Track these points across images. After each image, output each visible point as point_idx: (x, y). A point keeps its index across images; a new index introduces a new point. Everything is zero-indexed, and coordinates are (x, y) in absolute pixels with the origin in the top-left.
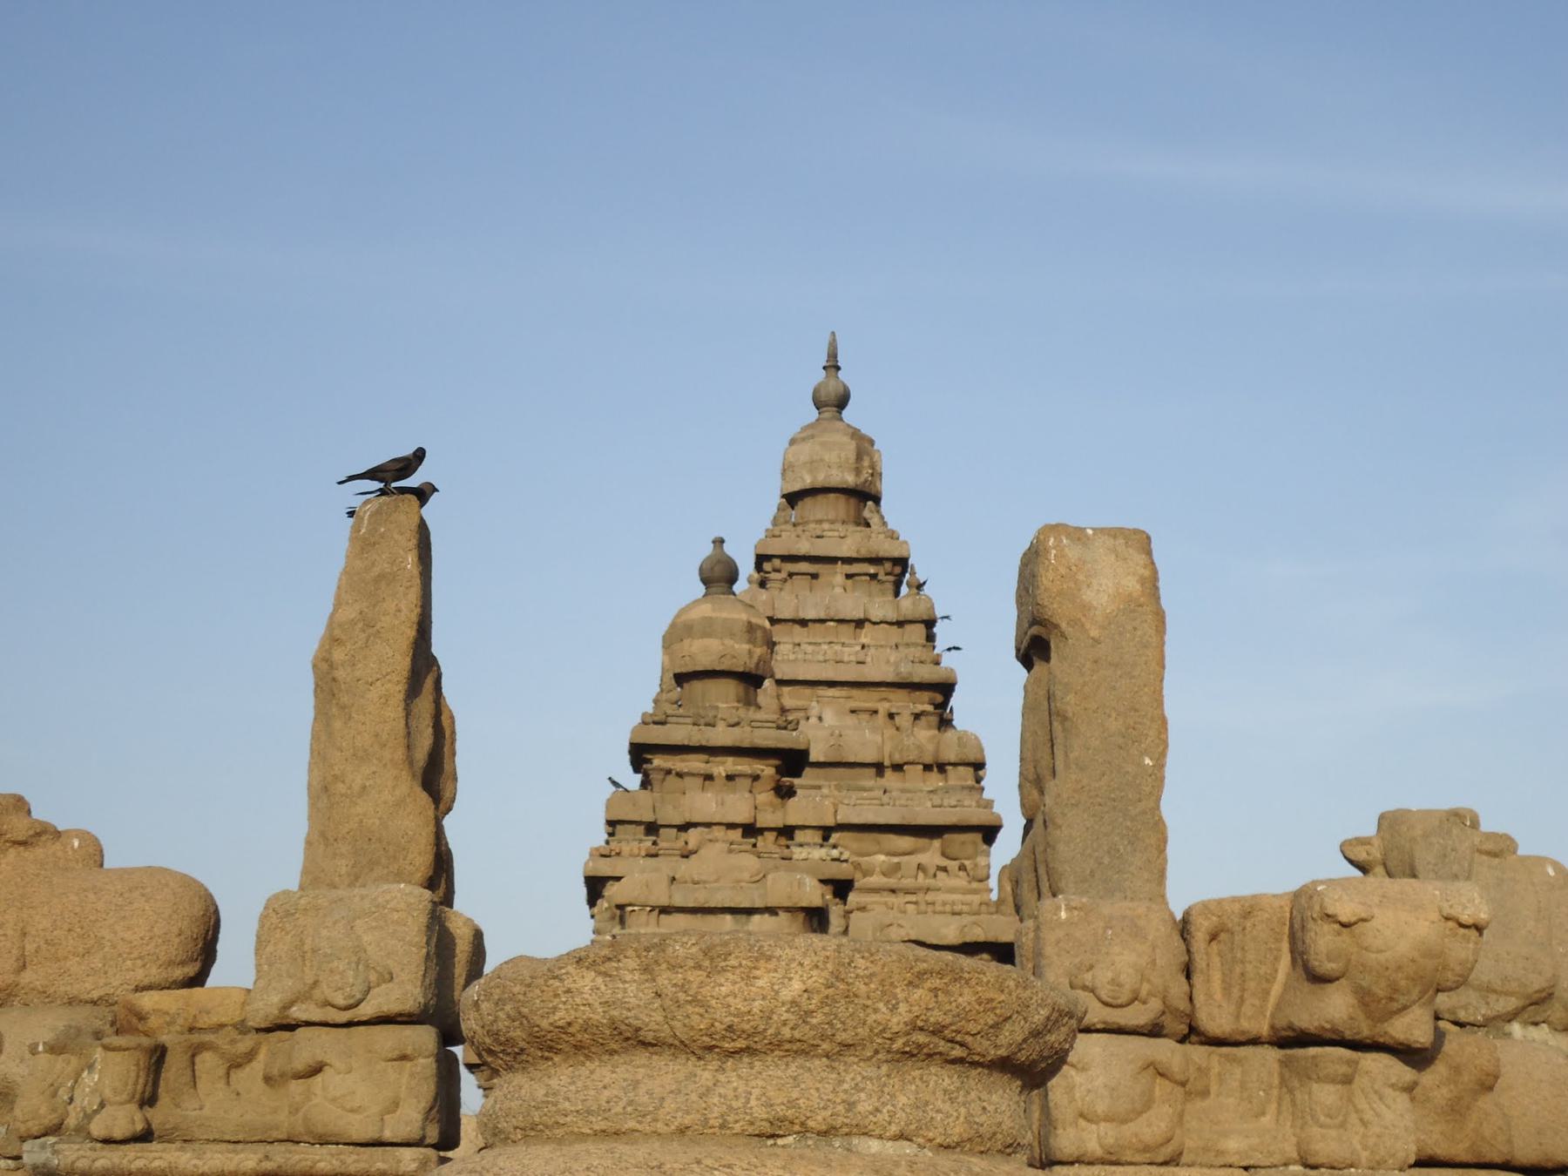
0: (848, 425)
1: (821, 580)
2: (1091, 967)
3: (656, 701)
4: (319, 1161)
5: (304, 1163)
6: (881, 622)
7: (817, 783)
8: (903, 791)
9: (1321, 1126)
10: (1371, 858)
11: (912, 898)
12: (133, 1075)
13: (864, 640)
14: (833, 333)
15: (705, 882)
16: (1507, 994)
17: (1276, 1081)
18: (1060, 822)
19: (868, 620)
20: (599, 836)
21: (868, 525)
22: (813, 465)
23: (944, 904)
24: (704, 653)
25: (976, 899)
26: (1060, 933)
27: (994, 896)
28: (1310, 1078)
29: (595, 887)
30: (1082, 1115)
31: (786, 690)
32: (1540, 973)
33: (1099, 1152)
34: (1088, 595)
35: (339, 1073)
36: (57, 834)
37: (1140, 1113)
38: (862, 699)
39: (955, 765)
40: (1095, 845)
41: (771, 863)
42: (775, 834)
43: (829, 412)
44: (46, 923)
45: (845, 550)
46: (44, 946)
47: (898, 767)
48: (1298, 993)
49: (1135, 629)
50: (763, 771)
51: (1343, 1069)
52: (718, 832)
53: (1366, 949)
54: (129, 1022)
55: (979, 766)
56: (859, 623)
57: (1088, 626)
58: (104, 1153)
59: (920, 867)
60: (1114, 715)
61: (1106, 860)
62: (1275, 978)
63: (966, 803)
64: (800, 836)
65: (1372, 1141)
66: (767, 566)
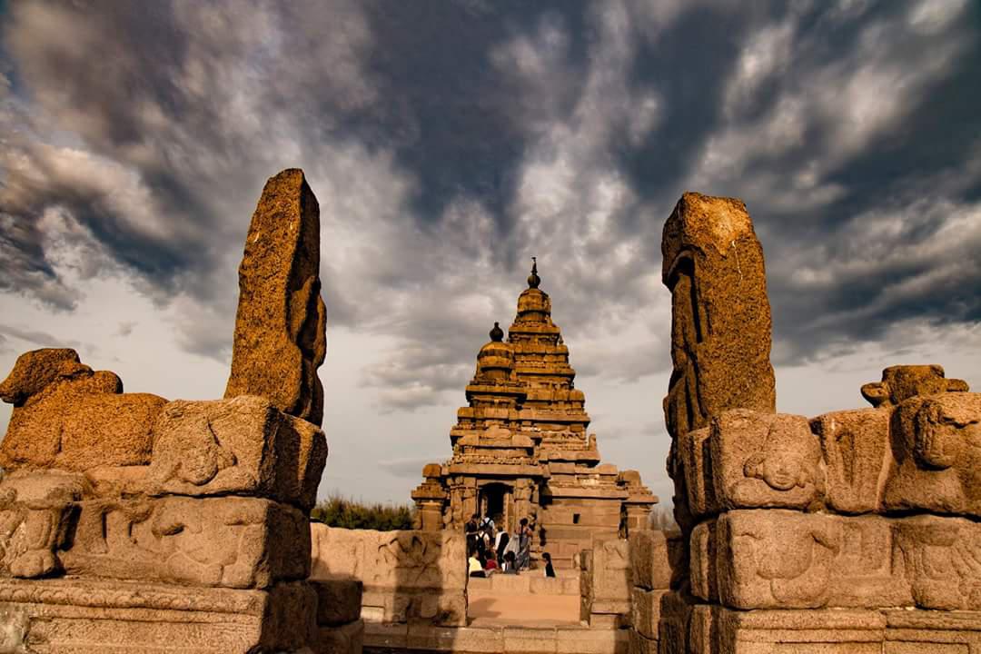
3: (475, 377)
4: (176, 598)
5: (164, 600)
9: (933, 578)
10: (882, 395)
12: (46, 528)
13: (545, 360)
17: (888, 541)
20: (455, 422)
25: (581, 446)
26: (735, 436)
28: (924, 542)
29: (454, 439)
30: (758, 573)
33: (773, 602)
34: (717, 231)
35: (192, 533)
36: (91, 373)
37: (802, 572)
40: (731, 383)
44: (74, 424)
45: (539, 330)
46: (71, 439)
48: (909, 478)
49: (746, 251)
53: (974, 445)
55: (583, 402)
57: (718, 248)
58: (21, 586)
59: (563, 435)
60: (738, 301)
61: (739, 392)
62: (881, 467)
64: (524, 423)
65: (969, 589)
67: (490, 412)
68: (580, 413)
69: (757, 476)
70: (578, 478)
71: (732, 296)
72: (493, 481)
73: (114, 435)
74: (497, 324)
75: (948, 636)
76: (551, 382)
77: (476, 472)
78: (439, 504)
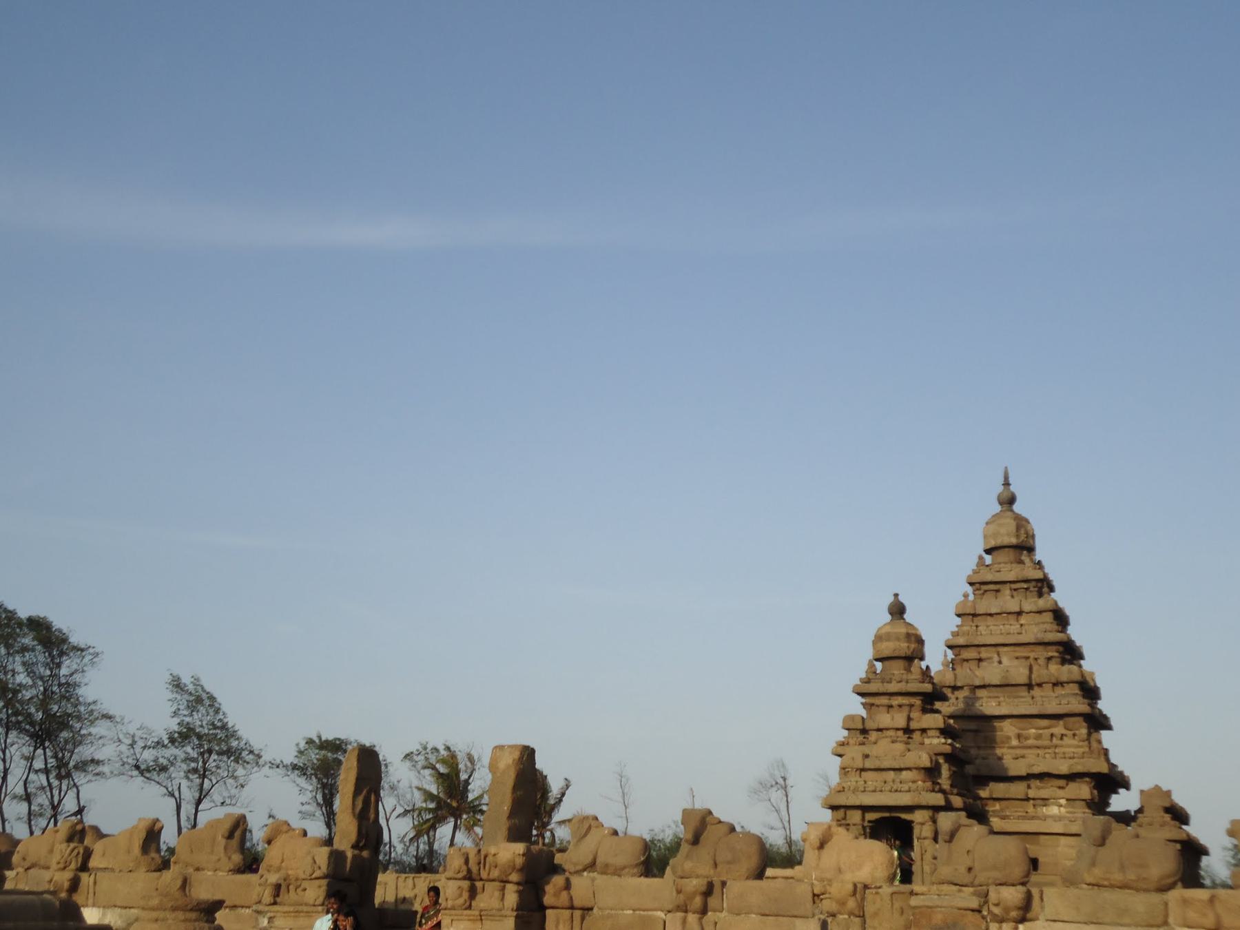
6: (1031, 612)
7: (996, 695)
13: (1022, 622)
14: (1006, 468)
19: (1023, 612)
22: (995, 535)
23: (1064, 753)
24: (888, 648)
31: (983, 649)
38: (1022, 652)
39: (1068, 683)
43: (1005, 508)
45: (1011, 577)
47: (1040, 685)
52: (891, 733)
56: (1019, 613)
59: (1052, 735)
64: (930, 733)
67: (885, 719)
70: (1034, 806)
72: (887, 815)
74: (896, 595)
75: (497, 918)
76: (1032, 655)
77: (858, 803)
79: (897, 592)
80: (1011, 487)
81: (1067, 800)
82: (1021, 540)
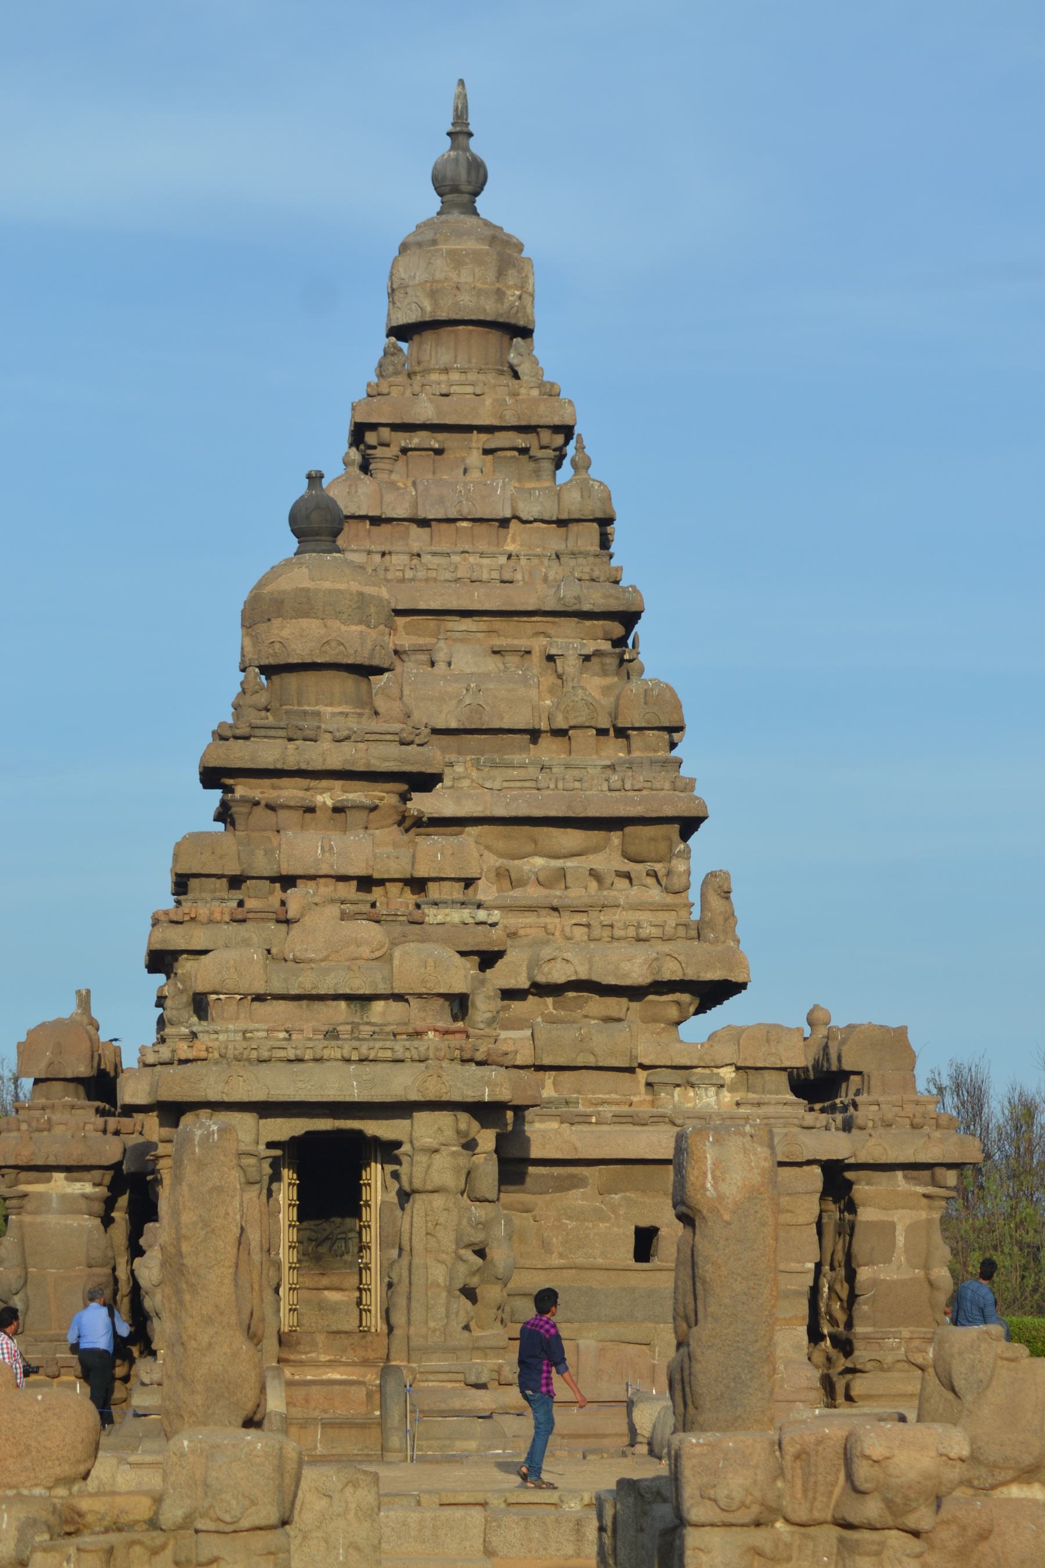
0: (487, 224)
1: (448, 456)
2: (714, 1486)
3: (236, 707)
6: (536, 520)
8: (568, 767)
11: (583, 919)
13: (510, 547)
14: (461, 82)
15: (311, 961)
16: (1008, 1468)
17: (835, 1550)
18: (700, 1358)
19: (516, 517)
21: (516, 375)
25: (671, 919)
26: (695, 1461)
27: (696, 915)
32: (1030, 1454)
40: (725, 1375)
41: (397, 930)
42: (401, 884)
47: (560, 733)
50: (382, 799)
51: (875, 1548)
52: (327, 889)
54: (73, 1518)
56: (504, 523)
57: (722, 1212)
59: (593, 874)
61: (732, 1385)
63: (657, 785)
66: (371, 438)
68: (663, 780)
69: (710, 1499)
70: (649, 1085)
71: (733, 1273)
73: (45, 1447)
76: (538, 645)
78: (88, 1188)
79: (315, 467)
80: (472, 140)
81: (738, 1068)
82: (506, 305)
